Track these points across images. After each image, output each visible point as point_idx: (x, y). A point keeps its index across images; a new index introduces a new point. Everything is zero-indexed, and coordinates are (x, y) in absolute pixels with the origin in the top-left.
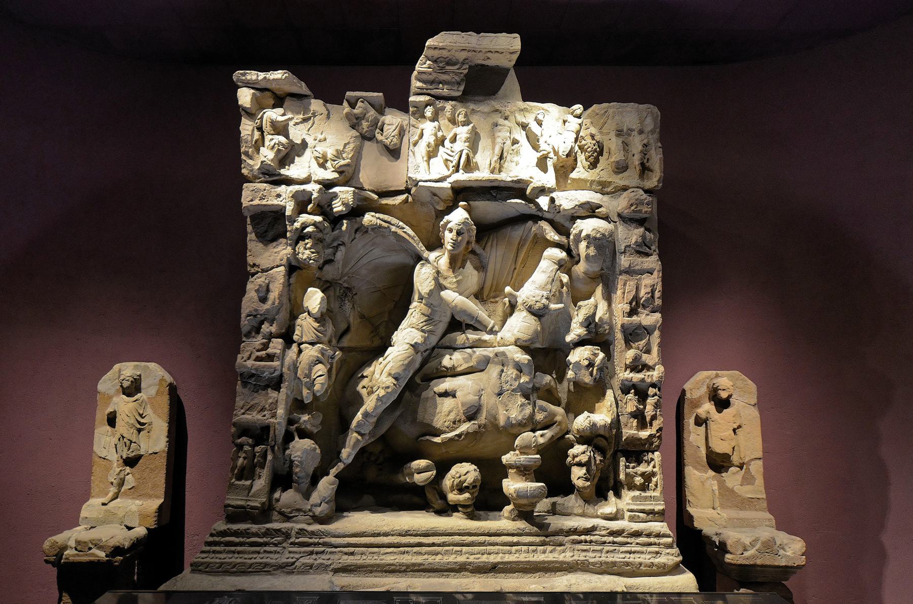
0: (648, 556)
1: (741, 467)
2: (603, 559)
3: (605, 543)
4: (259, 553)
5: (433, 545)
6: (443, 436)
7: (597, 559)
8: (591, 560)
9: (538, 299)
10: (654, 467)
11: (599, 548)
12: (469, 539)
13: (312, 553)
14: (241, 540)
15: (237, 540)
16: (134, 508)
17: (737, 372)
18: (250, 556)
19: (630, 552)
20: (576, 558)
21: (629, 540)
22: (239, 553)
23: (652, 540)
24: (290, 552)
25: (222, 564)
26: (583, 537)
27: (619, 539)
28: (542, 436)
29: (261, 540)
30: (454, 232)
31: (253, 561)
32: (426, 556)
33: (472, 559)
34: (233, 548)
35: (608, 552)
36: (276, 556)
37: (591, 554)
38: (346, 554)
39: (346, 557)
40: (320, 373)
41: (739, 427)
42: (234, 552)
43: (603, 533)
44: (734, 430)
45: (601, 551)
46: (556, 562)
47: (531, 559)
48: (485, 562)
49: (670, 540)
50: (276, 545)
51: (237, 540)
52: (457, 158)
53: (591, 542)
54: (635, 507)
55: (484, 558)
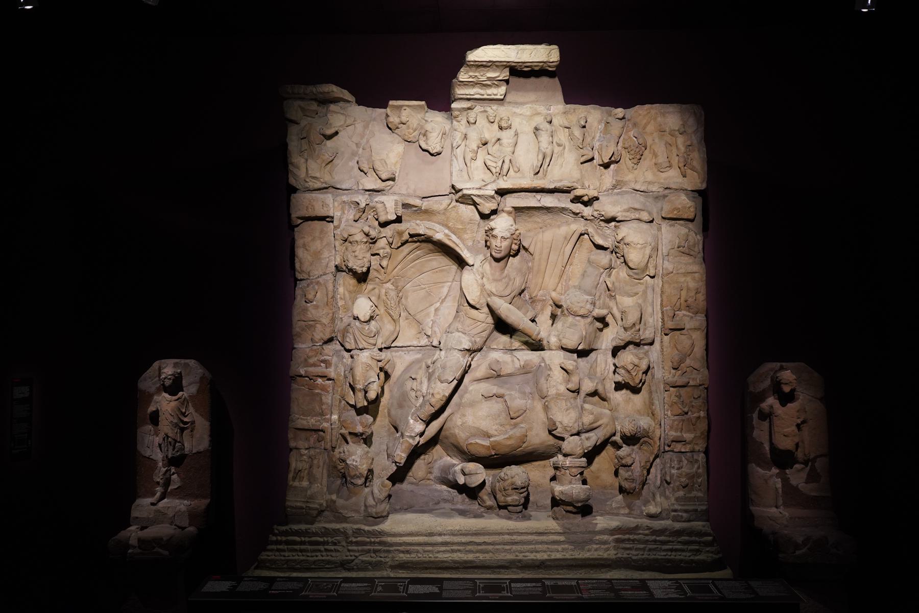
0: (688, 554)
1: (806, 463)
2: (645, 556)
3: (647, 541)
4: (320, 551)
5: (485, 543)
6: (492, 439)
7: (640, 556)
8: (634, 558)
9: (582, 304)
10: (699, 468)
11: (642, 546)
12: (519, 538)
13: (369, 551)
14: (303, 539)
15: (298, 539)
16: (183, 508)
17: (803, 364)
18: (314, 554)
19: (671, 550)
20: (619, 555)
21: (671, 539)
22: (301, 551)
23: (693, 538)
24: (349, 551)
25: (288, 561)
26: (627, 536)
27: (662, 538)
28: (587, 439)
29: (321, 540)
30: (499, 241)
31: (315, 558)
32: (478, 555)
33: (521, 557)
34: (295, 547)
35: (650, 550)
36: (338, 554)
37: (634, 552)
38: (403, 552)
39: (402, 555)
40: (372, 380)
41: (804, 422)
42: (296, 550)
43: (647, 532)
44: (798, 426)
45: (644, 549)
46: (601, 559)
47: (577, 557)
48: (532, 560)
49: (710, 538)
50: (335, 544)
51: (298, 539)
52: (500, 164)
53: (633, 540)
54: (679, 508)
55: (532, 556)
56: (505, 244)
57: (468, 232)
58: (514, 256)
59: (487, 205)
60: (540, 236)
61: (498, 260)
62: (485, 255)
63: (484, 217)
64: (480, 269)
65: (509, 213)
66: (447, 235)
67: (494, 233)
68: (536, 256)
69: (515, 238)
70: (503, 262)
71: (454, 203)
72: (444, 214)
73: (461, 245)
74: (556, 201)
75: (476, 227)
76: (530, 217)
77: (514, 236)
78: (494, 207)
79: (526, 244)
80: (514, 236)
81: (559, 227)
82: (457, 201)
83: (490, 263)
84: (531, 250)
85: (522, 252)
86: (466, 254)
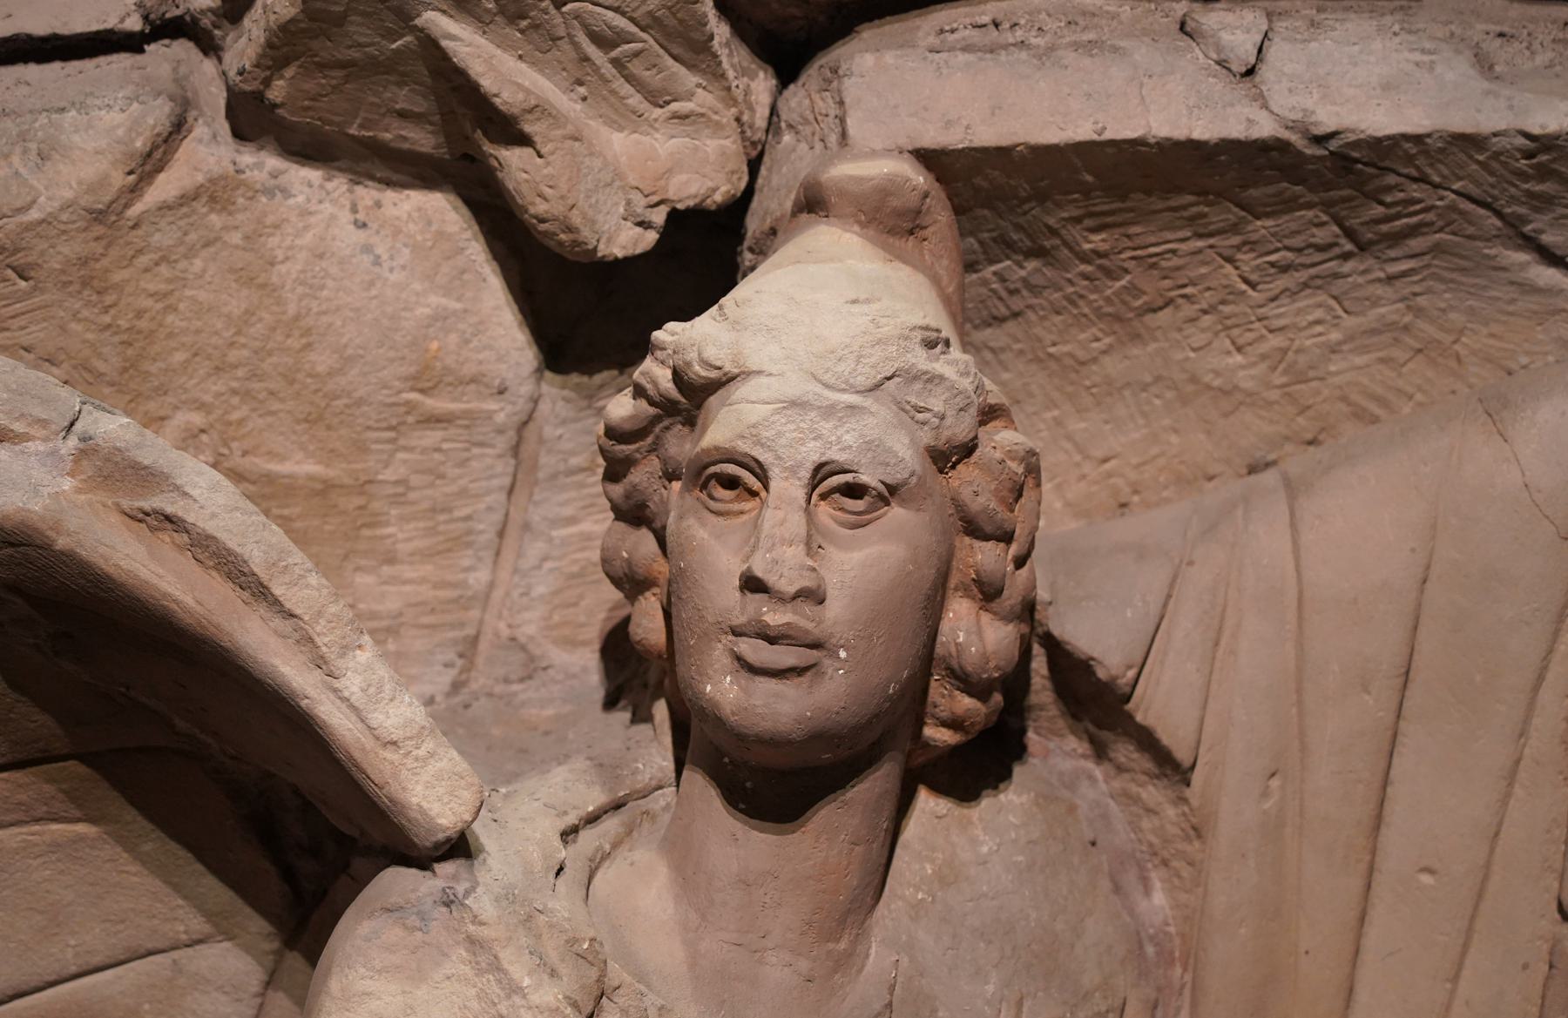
56: (862, 565)
57: (401, 533)
58: (981, 764)
59: (619, 143)
60: (1267, 536)
61: (771, 783)
62: (606, 769)
63: (590, 309)
64: (562, 903)
65: (892, 222)
66: (114, 472)
67: (724, 427)
68: (1231, 786)
69: (970, 504)
70: (837, 825)
71: (209, 151)
72: (87, 279)
73: (303, 589)
74: (1456, 70)
75: (492, 467)
76: (1127, 322)
77: (973, 485)
78: (699, 169)
79: (1096, 632)
80: (973, 485)
81: (1495, 410)
82: (250, 118)
83: (688, 874)
84: (1163, 705)
85: (1055, 751)
86: (376, 708)
